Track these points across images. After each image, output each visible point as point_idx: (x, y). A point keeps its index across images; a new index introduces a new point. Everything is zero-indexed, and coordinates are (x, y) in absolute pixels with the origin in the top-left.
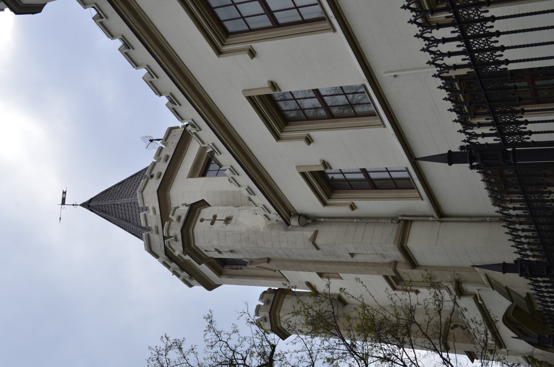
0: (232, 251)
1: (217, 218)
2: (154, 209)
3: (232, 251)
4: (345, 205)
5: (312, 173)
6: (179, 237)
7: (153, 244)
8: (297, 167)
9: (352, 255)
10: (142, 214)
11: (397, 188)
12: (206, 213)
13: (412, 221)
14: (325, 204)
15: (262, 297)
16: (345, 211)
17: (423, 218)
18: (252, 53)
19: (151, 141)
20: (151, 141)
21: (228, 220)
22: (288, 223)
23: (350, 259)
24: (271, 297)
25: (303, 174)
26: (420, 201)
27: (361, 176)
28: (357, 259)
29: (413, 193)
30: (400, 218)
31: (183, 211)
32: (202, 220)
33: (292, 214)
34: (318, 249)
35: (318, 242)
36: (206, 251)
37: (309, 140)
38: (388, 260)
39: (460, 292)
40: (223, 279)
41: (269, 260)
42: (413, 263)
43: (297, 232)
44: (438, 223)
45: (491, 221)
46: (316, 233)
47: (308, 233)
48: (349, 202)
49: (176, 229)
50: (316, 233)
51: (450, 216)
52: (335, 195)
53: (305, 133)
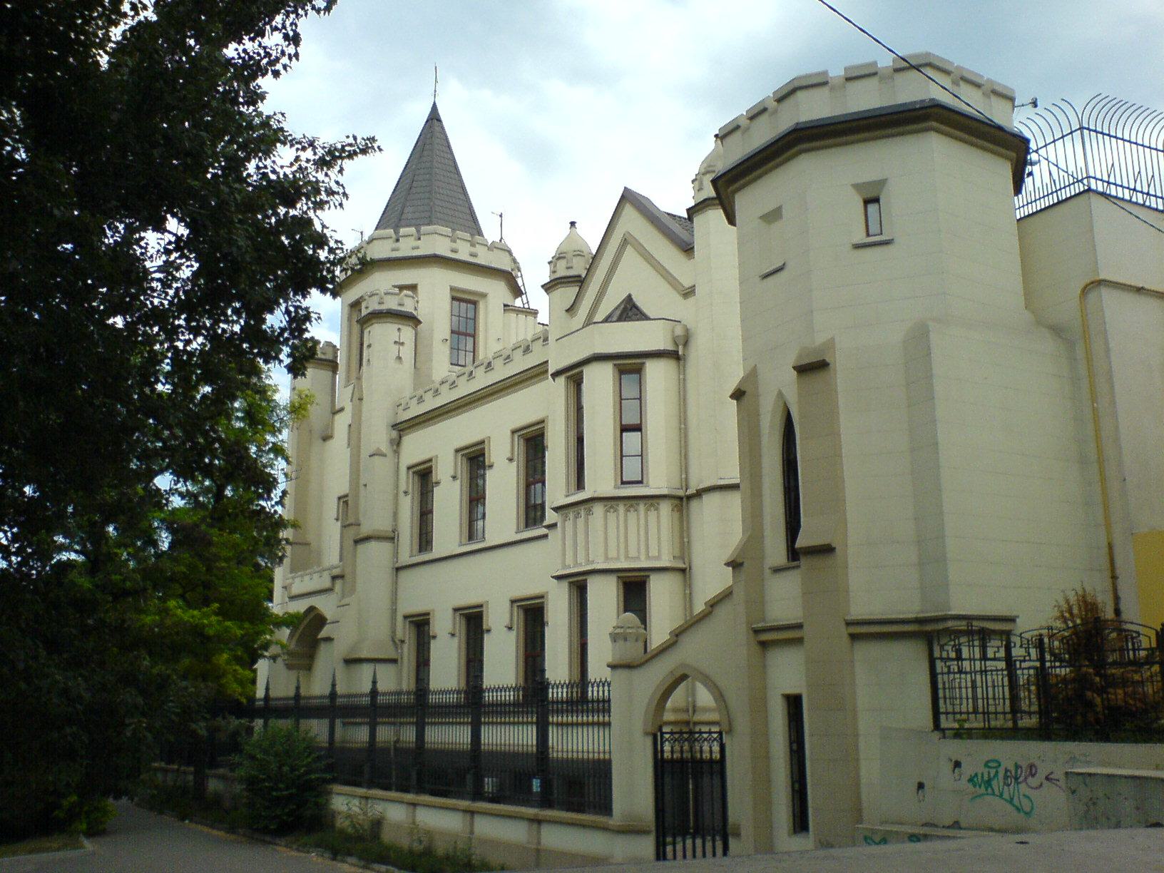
0: (369, 360)
1: (401, 347)
2: (418, 248)
3: (369, 360)
4: (408, 486)
5: (431, 467)
6: (384, 307)
7: (380, 242)
8: (437, 456)
9: (365, 485)
10: (412, 230)
11: (421, 535)
12: (407, 333)
13: (394, 543)
14: (409, 468)
15: (329, 344)
16: (403, 487)
17: (396, 554)
18: (511, 460)
19: (501, 216)
20: (501, 216)
21: (399, 358)
22: (394, 426)
23: (362, 482)
24: (330, 357)
25: (430, 460)
26: (407, 554)
27: (429, 506)
28: (362, 488)
29: (416, 547)
30: (396, 533)
31: (408, 307)
32: (399, 329)
33: (401, 433)
34: (370, 456)
35: (376, 457)
36: (370, 332)
37: (454, 477)
38: (361, 519)
39: (334, 578)
40: (347, 309)
41: (361, 399)
42: (357, 542)
43: (385, 435)
44: (392, 566)
45: (392, 609)
46: (385, 455)
47: (385, 447)
48: (410, 491)
49: (391, 304)
50: (385, 455)
51: (396, 575)
52: (416, 478)
53: (459, 476)
